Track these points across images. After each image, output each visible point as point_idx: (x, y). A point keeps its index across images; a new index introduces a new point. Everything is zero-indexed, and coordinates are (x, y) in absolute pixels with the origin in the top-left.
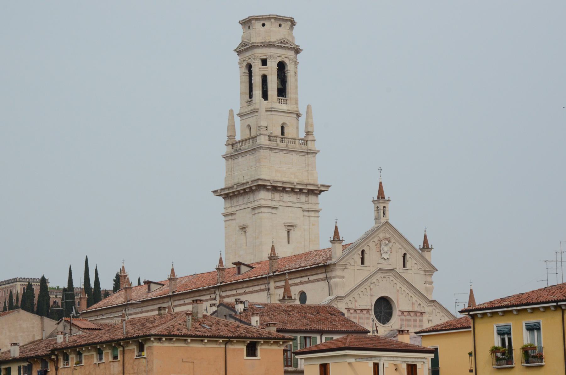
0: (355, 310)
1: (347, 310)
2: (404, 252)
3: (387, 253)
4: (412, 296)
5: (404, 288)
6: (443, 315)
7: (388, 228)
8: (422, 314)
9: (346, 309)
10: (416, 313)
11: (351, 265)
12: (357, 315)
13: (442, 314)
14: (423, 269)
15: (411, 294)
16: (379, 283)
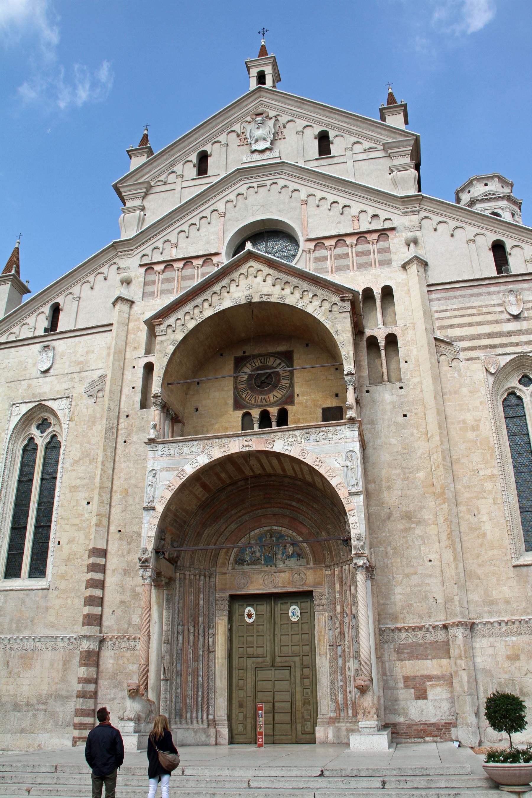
0: (169, 264)
1: (143, 269)
2: (317, 129)
3: (264, 139)
4: (348, 202)
5: (319, 194)
6: (459, 224)
7: (268, 98)
8: (388, 236)
9: (141, 266)
10: (366, 235)
11: (165, 183)
12: (176, 274)
13: (453, 224)
14: (382, 148)
15: (343, 201)
16: (246, 198)
